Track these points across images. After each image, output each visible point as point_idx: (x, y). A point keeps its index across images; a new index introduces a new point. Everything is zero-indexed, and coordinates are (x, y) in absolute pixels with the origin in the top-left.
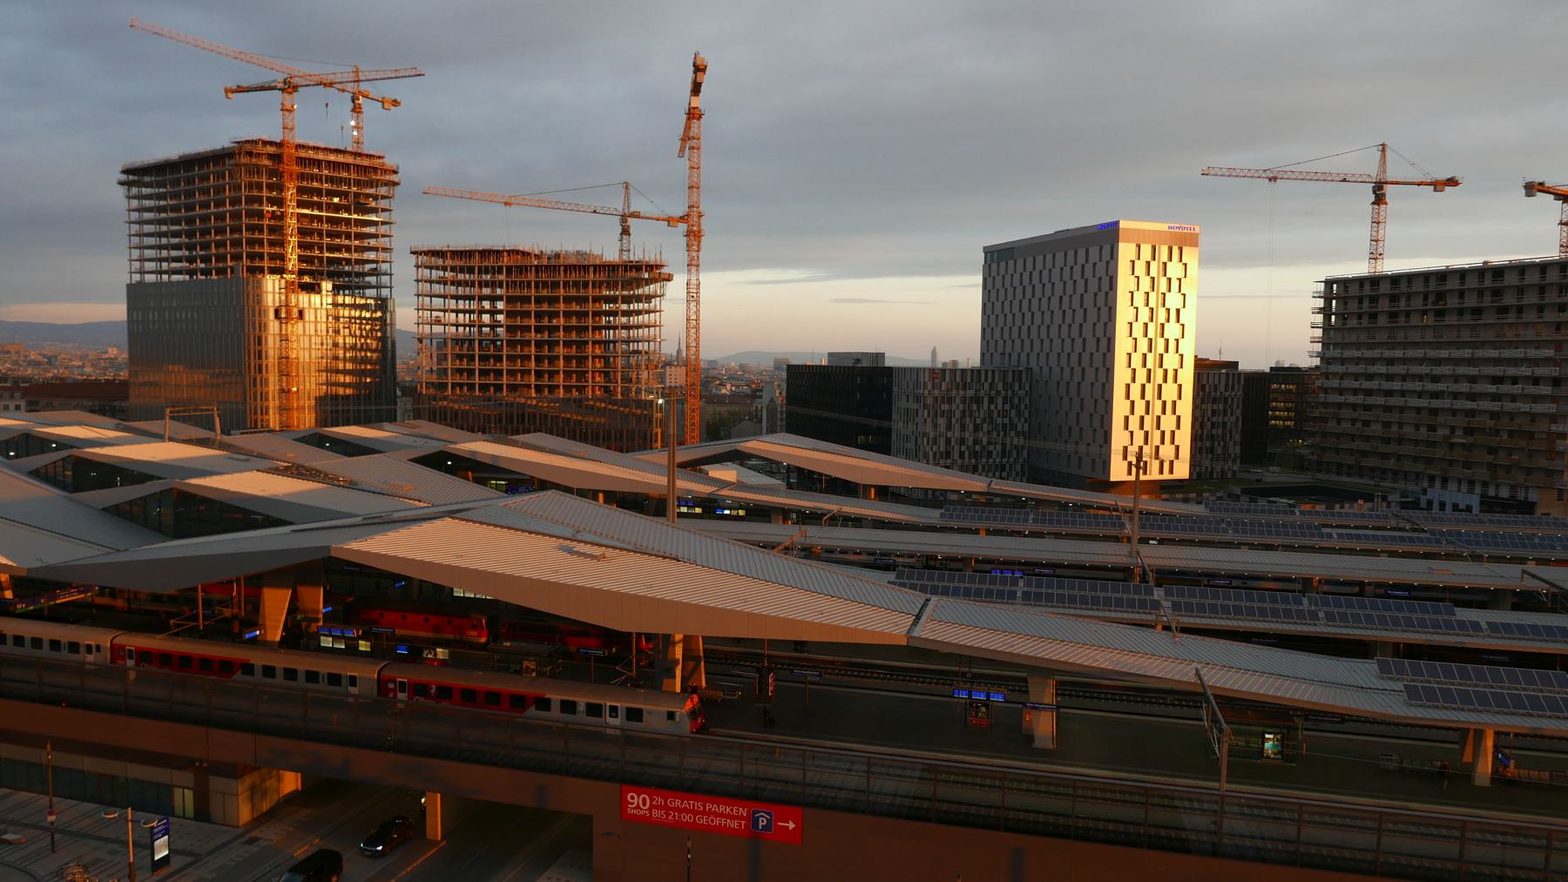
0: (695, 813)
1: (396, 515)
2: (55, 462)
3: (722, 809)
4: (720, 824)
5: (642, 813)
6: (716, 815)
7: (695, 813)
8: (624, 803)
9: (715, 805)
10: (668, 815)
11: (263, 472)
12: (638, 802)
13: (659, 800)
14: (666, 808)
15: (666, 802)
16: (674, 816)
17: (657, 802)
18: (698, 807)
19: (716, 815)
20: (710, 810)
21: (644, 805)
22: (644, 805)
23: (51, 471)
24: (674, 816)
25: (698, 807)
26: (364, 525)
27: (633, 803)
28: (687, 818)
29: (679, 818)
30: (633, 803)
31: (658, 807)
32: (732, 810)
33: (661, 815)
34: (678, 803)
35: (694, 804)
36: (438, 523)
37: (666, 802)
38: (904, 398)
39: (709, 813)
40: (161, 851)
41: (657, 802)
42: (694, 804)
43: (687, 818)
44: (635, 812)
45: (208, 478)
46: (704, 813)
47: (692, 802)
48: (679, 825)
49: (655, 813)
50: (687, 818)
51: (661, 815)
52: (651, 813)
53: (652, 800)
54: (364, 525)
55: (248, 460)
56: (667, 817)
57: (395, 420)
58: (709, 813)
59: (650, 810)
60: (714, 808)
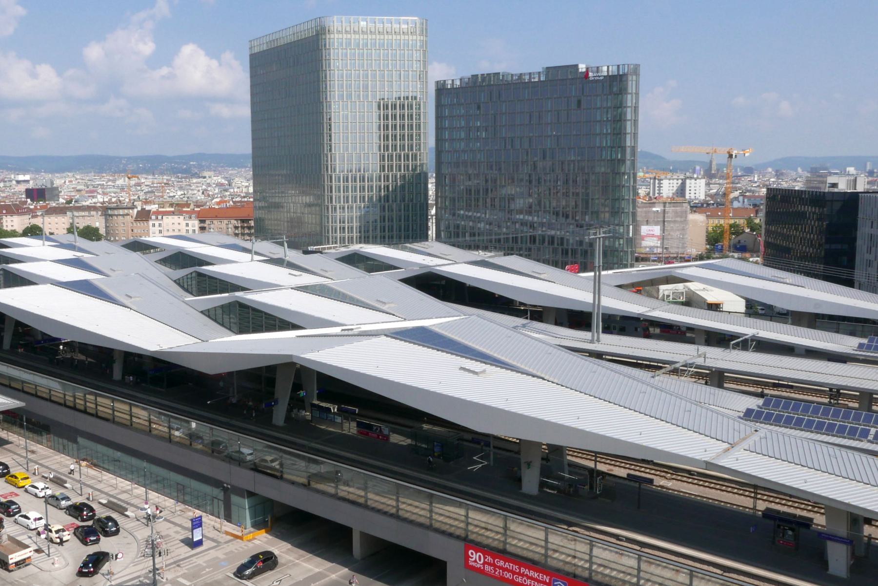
0: (514, 573)
1: (364, 328)
2: (187, 275)
3: (532, 573)
4: (530, 585)
5: (478, 566)
6: (528, 577)
7: (514, 573)
8: (467, 557)
9: (527, 570)
10: (496, 571)
11: (295, 289)
12: (476, 558)
13: (489, 559)
14: (493, 565)
15: (494, 561)
16: (499, 573)
17: (488, 560)
18: (516, 569)
19: (528, 577)
20: (524, 572)
21: (480, 560)
22: (480, 560)
23: (181, 281)
24: (499, 573)
25: (516, 569)
26: (341, 336)
27: (472, 558)
28: (508, 575)
29: (503, 574)
30: (472, 558)
31: (489, 564)
32: (539, 576)
33: (491, 570)
34: (501, 563)
35: (513, 566)
36: (374, 340)
37: (494, 561)
38: (869, 224)
39: (523, 575)
40: (197, 537)
41: (488, 560)
42: (513, 566)
43: (508, 575)
44: (474, 564)
45: (264, 294)
46: (519, 574)
47: (511, 565)
48: (503, 579)
49: (488, 568)
50: (508, 575)
51: (491, 570)
52: (484, 567)
53: (485, 558)
54: (341, 336)
55: (301, 275)
56: (494, 573)
57: (424, 237)
58: (523, 575)
59: (485, 563)
60: (527, 572)
